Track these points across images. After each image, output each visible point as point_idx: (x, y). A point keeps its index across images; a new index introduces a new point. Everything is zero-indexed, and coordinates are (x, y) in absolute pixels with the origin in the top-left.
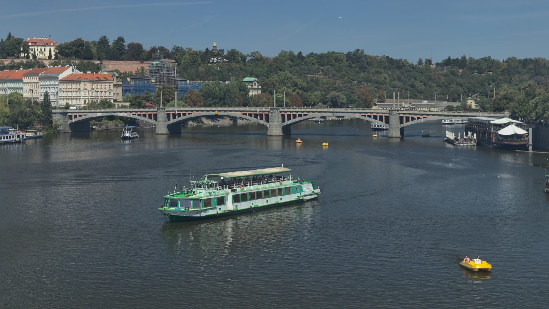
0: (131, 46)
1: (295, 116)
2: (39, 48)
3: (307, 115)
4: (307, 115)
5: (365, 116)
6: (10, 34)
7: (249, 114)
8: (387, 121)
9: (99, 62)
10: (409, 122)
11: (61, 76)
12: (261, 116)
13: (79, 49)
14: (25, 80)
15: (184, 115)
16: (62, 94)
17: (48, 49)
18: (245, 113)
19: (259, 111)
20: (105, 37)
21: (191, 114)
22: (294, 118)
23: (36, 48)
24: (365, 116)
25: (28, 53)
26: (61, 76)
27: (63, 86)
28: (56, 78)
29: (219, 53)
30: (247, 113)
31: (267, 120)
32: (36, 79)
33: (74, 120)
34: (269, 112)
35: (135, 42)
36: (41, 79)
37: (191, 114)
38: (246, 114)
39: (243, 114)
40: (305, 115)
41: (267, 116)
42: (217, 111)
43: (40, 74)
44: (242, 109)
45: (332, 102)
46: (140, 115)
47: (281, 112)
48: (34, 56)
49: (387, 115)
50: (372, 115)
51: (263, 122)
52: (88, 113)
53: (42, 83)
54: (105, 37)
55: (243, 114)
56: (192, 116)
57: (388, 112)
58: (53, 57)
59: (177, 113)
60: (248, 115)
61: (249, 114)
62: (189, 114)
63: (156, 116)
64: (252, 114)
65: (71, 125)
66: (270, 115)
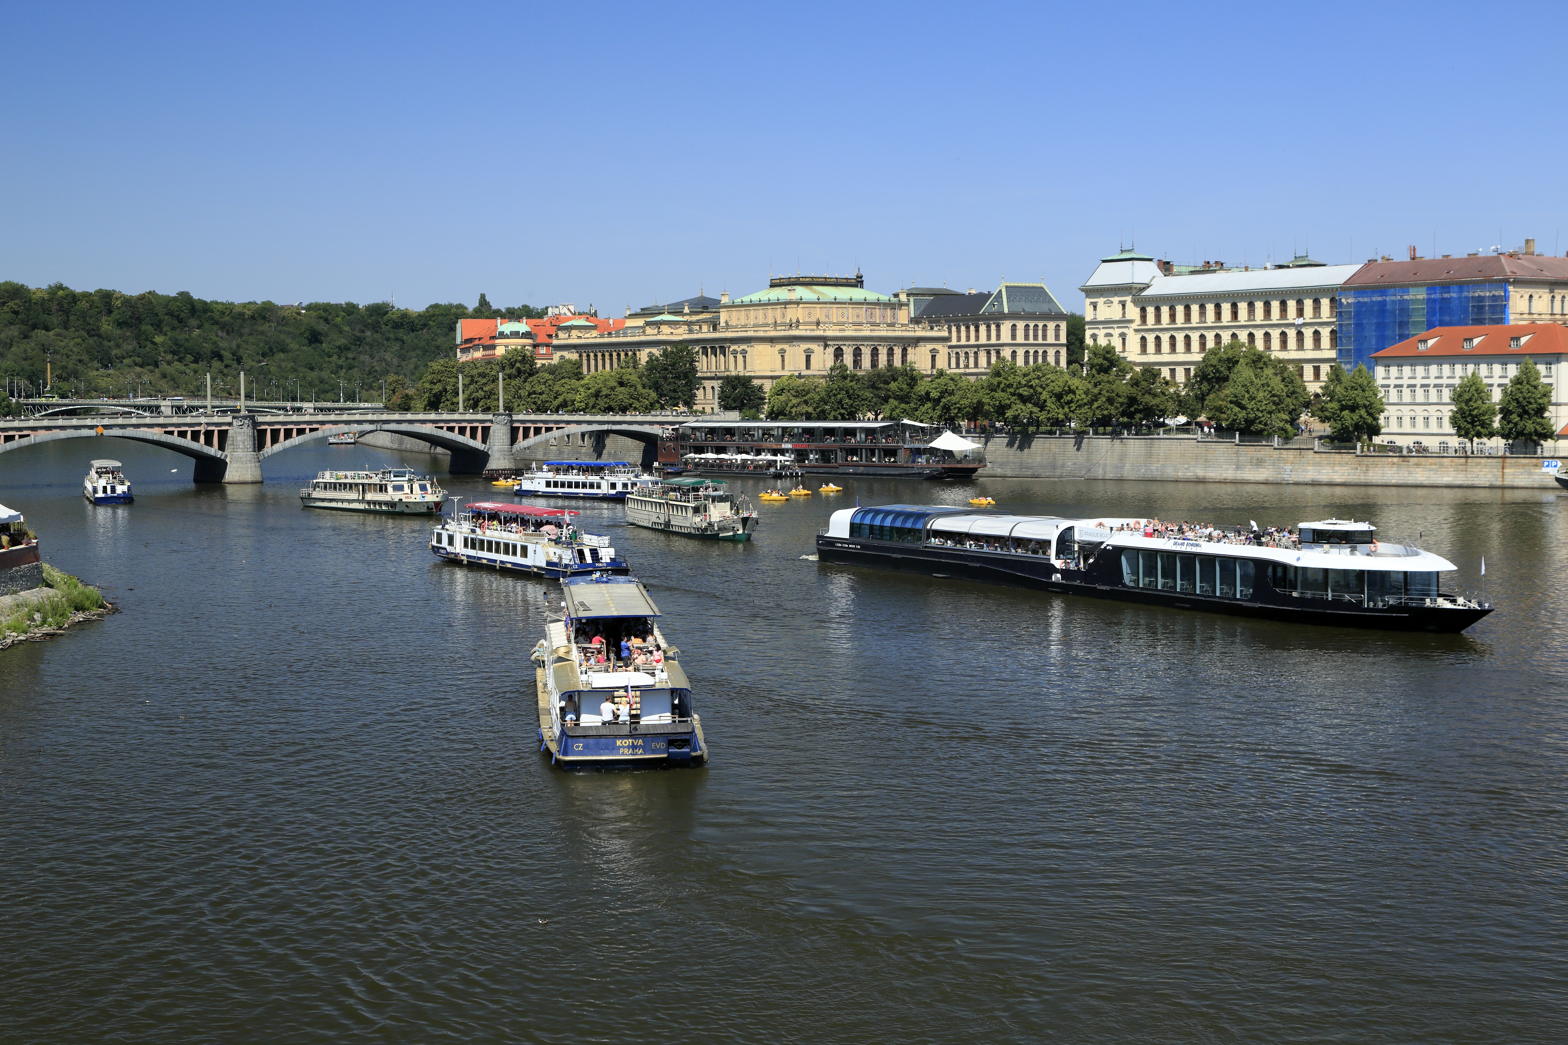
1: (288, 434)
3: (317, 429)
4: (317, 429)
5: (442, 428)
7: (179, 432)
18: (170, 429)
19: (207, 424)
21: (28, 435)
31: (222, 447)
34: (230, 424)
37: (28, 435)
38: (171, 433)
39: (166, 432)
40: (311, 430)
41: (223, 435)
50: (457, 426)
51: (213, 451)
55: (166, 432)
56: (33, 442)
60: (176, 434)
61: (179, 432)
62: (21, 437)
64: (186, 432)
66: (230, 433)
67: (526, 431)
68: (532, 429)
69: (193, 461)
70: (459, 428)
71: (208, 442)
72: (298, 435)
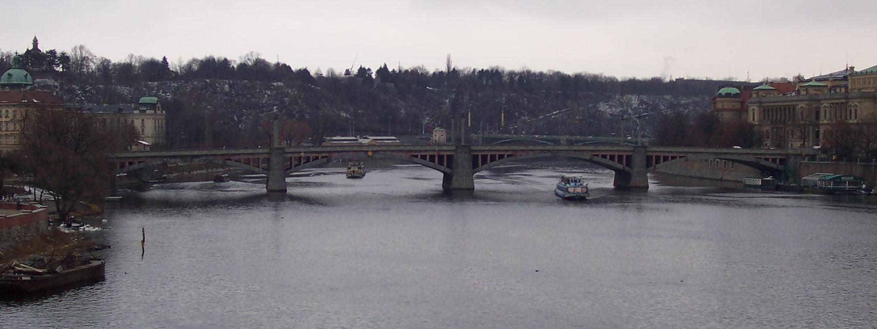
3: (511, 155)
5: (597, 155)
7: (421, 155)
10: (661, 164)
12: (441, 158)
22: (491, 161)
24: (597, 155)
30: (419, 154)
38: (417, 156)
42: (372, 151)
47: (472, 151)
49: (629, 154)
50: (608, 154)
52: (147, 157)
57: (632, 149)
59: (303, 154)
60: (419, 156)
64: (426, 156)
67: (658, 158)
68: (662, 158)
69: (443, 174)
70: (610, 156)
71: (441, 162)
72: (499, 159)
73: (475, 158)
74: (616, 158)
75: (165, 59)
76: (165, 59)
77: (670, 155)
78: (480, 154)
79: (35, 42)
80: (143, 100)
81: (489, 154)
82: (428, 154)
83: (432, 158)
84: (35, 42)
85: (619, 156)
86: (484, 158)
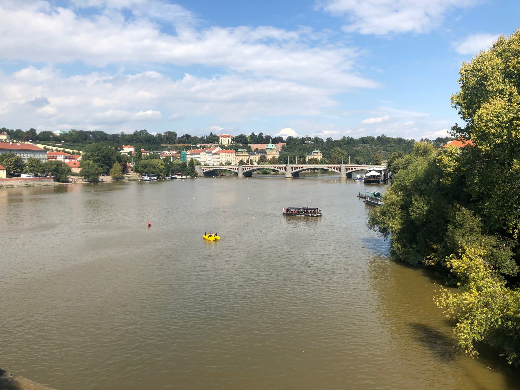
0: (266, 137)
2: (224, 139)
6: (211, 133)
8: (340, 170)
9: (250, 145)
11: (214, 152)
12: (283, 168)
13: (242, 139)
14: (201, 153)
15: (250, 168)
16: (214, 160)
17: (228, 139)
20: (253, 133)
23: (222, 139)
25: (219, 142)
26: (214, 152)
27: (214, 156)
28: (211, 153)
29: (309, 139)
32: (205, 153)
33: (204, 171)
35: (268, 135)
36: (207, 153)
41: (285, 168)
43: (206, 151)
44: (274, 165)
45: (356, 162)
46: (231, 168)
48: (221, 143)
50: (332, 167)
53: (207, 155)
54: (253, 133)
58: (230, 143)
63: (238, 169)
65: (204, 173)
73: (292, 168)
74: (335, 169)
75: (352, 137)
76: (352, 137)
77: (353, 167)
78: (293, 167)
79: (307, 136)
80: (314, 151)
81: (296, 167)
82: (279, 167)
83: (280, 168)
84: (307, 136)
85: (336, 168)
86: (295, 168)
